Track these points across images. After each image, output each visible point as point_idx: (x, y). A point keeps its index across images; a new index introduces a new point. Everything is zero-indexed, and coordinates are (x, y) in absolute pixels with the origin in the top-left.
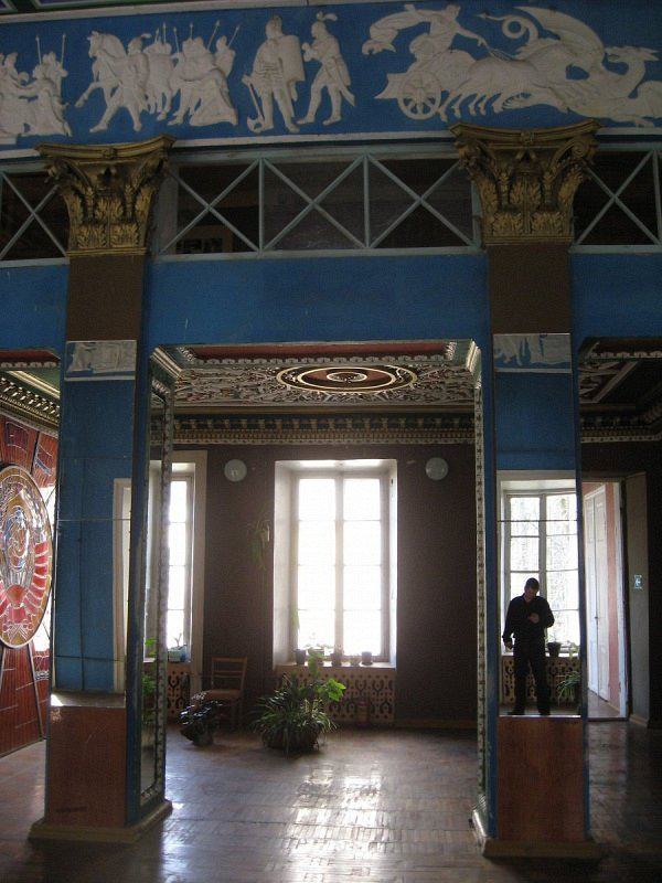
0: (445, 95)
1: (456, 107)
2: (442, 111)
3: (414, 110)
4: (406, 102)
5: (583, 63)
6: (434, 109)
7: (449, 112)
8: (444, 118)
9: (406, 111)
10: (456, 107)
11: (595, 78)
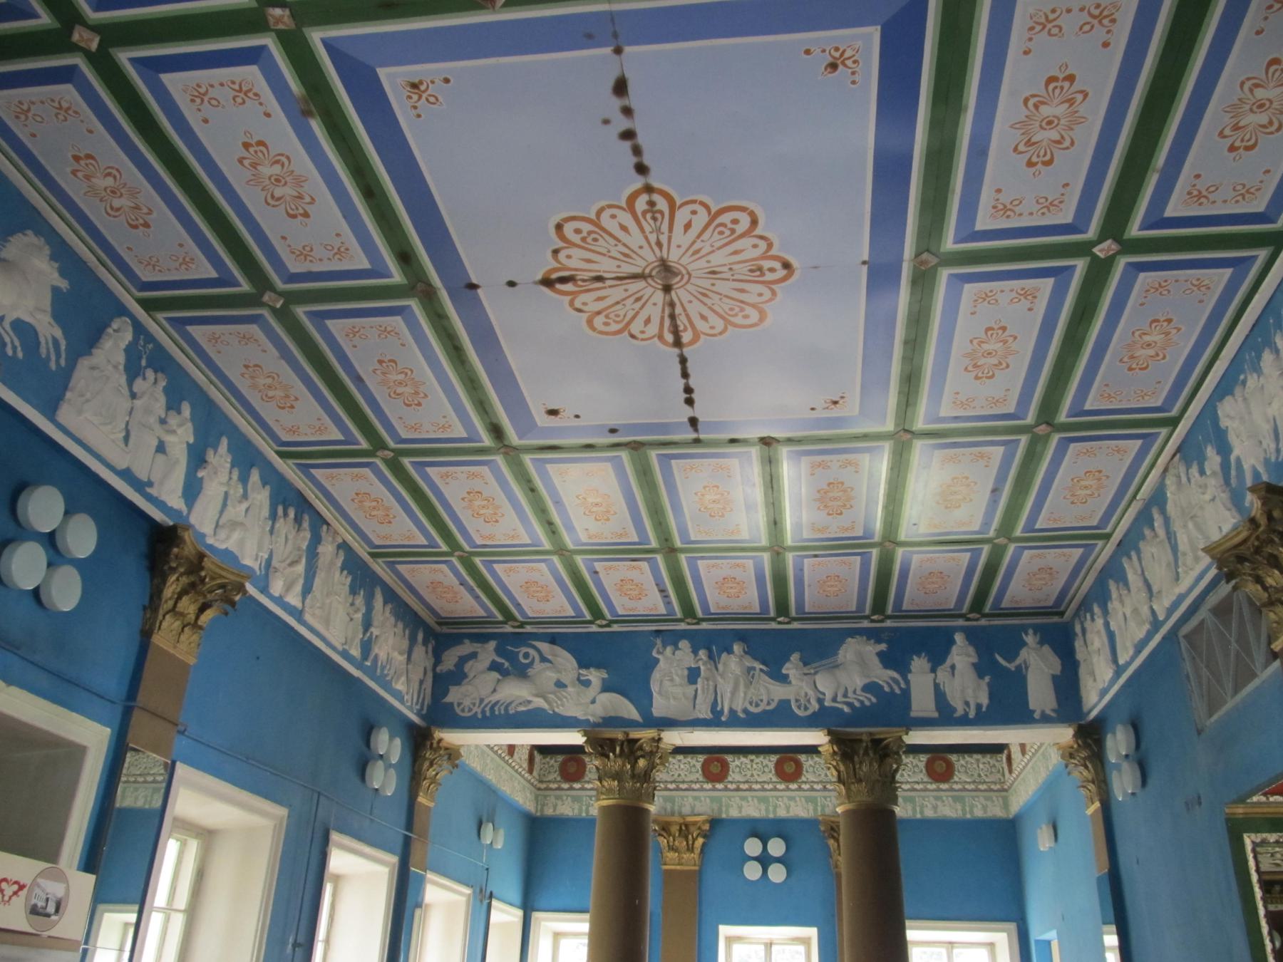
0: (482, 700)
1: (487, 709)
2: (479, 711)
3: (463, 711)
4: (459, 704)
5: (565, 680)
6: (475, 709)
7: (483, 712)
8: (480, 716)
9: (458, 710)
10: (487, 709)
11: (570, 689)
